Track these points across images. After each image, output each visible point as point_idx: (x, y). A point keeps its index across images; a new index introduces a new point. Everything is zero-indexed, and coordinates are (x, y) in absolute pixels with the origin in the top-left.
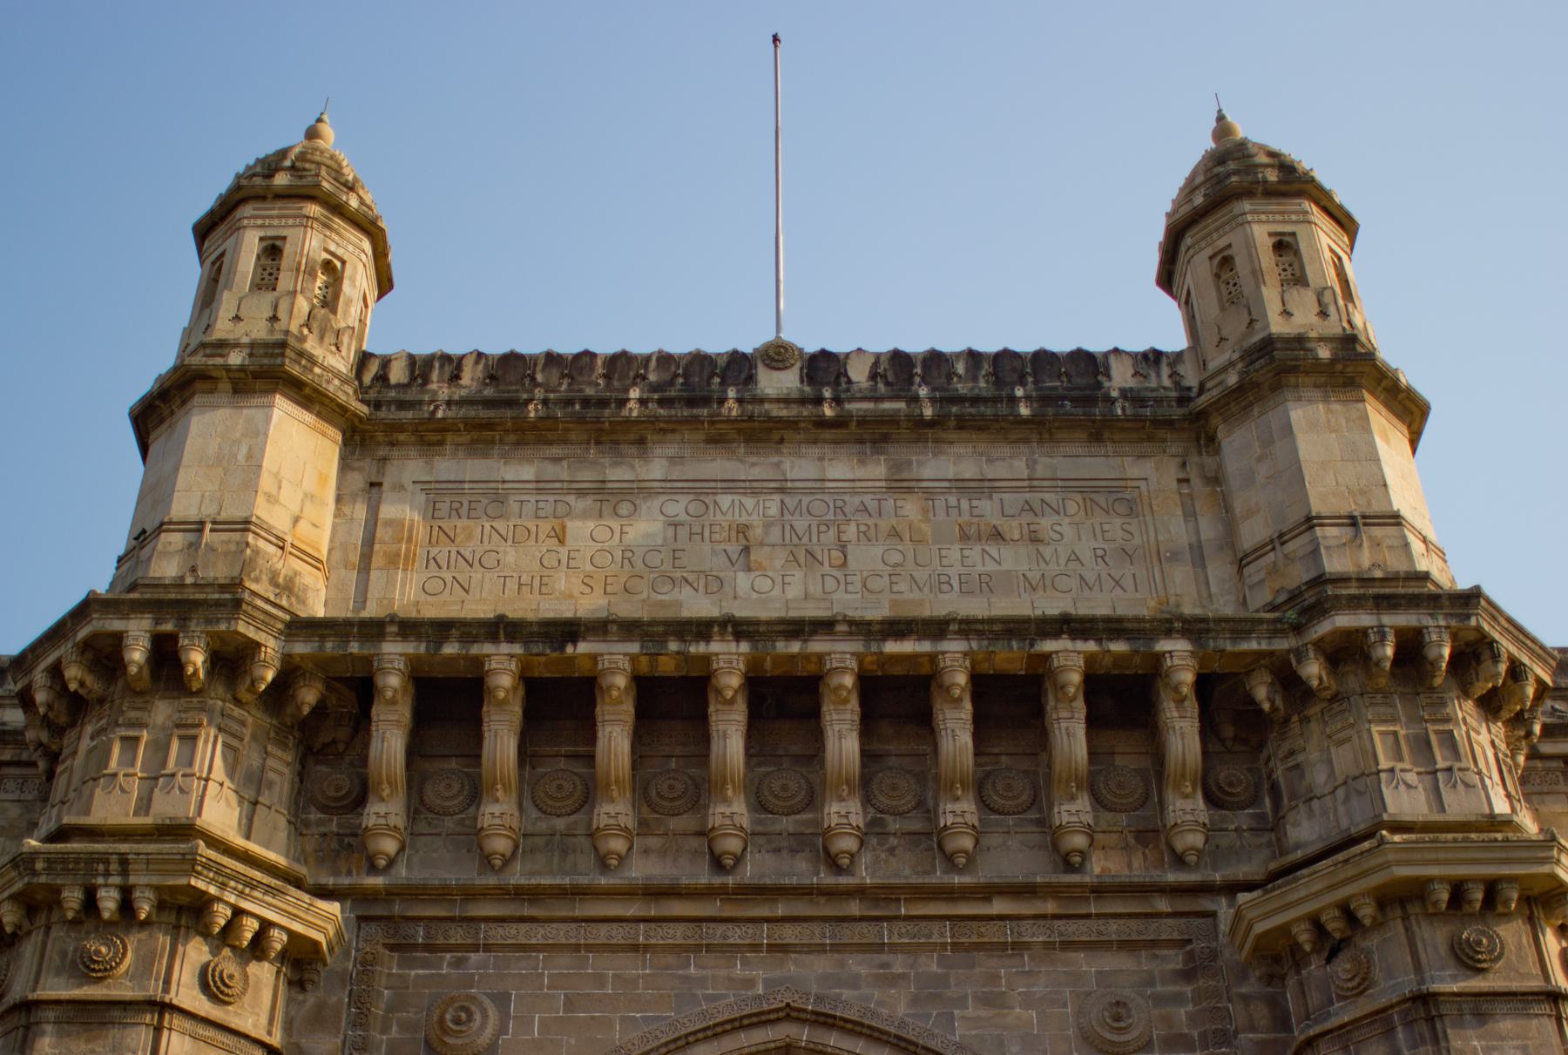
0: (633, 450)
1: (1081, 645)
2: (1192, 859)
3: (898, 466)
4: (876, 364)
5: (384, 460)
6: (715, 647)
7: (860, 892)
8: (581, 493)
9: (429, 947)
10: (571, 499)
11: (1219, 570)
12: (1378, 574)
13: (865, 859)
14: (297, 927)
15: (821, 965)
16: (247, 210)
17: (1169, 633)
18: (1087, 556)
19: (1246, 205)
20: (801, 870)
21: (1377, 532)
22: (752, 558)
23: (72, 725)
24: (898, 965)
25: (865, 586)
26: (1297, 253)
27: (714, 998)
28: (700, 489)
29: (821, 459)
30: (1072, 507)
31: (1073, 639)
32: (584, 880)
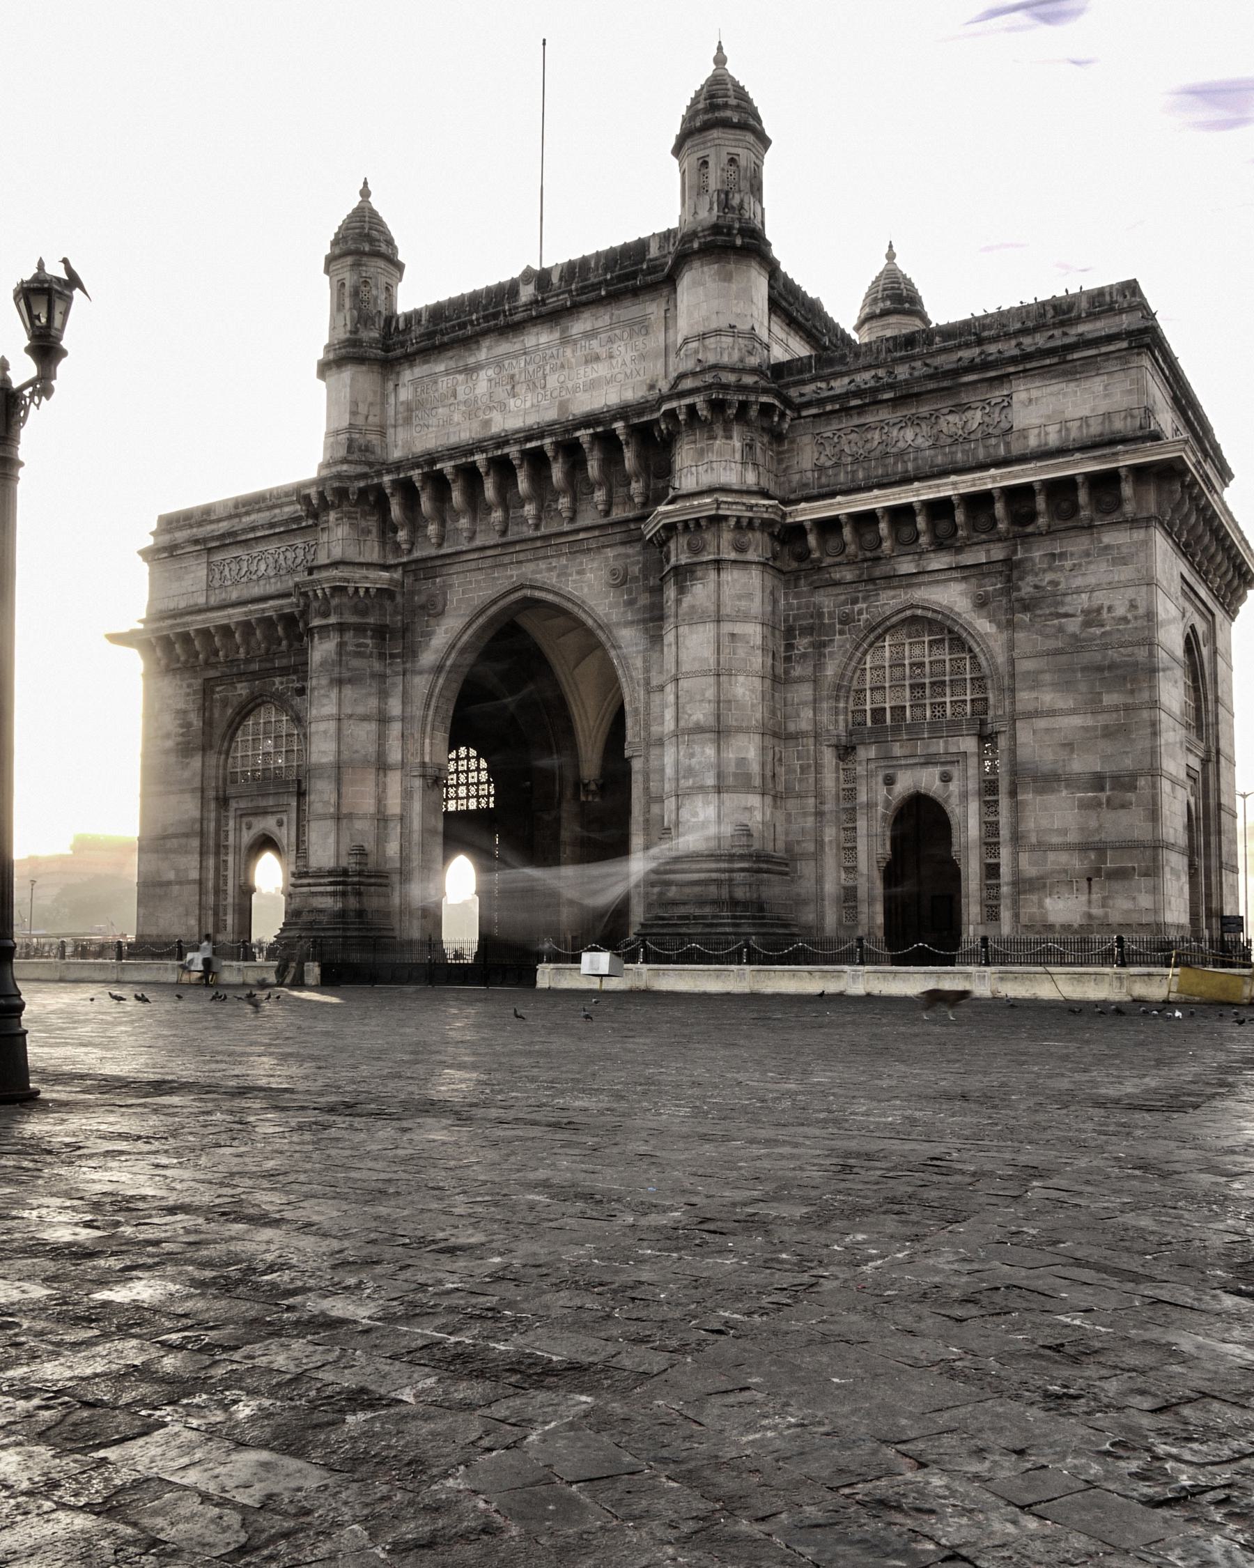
0: (474, 346)
3: (563, 331)
5: (398, 373)
6: (476, 457)
8: (460, 372)
13: (543, 523)
15: (531, 567)
17: (615, 419)
18: (628, 361)
19: (688, 144)
21: (707, 342)
24: (554, 562)
28: (498, 363)
30: (626, 335)
32: (459, 548)
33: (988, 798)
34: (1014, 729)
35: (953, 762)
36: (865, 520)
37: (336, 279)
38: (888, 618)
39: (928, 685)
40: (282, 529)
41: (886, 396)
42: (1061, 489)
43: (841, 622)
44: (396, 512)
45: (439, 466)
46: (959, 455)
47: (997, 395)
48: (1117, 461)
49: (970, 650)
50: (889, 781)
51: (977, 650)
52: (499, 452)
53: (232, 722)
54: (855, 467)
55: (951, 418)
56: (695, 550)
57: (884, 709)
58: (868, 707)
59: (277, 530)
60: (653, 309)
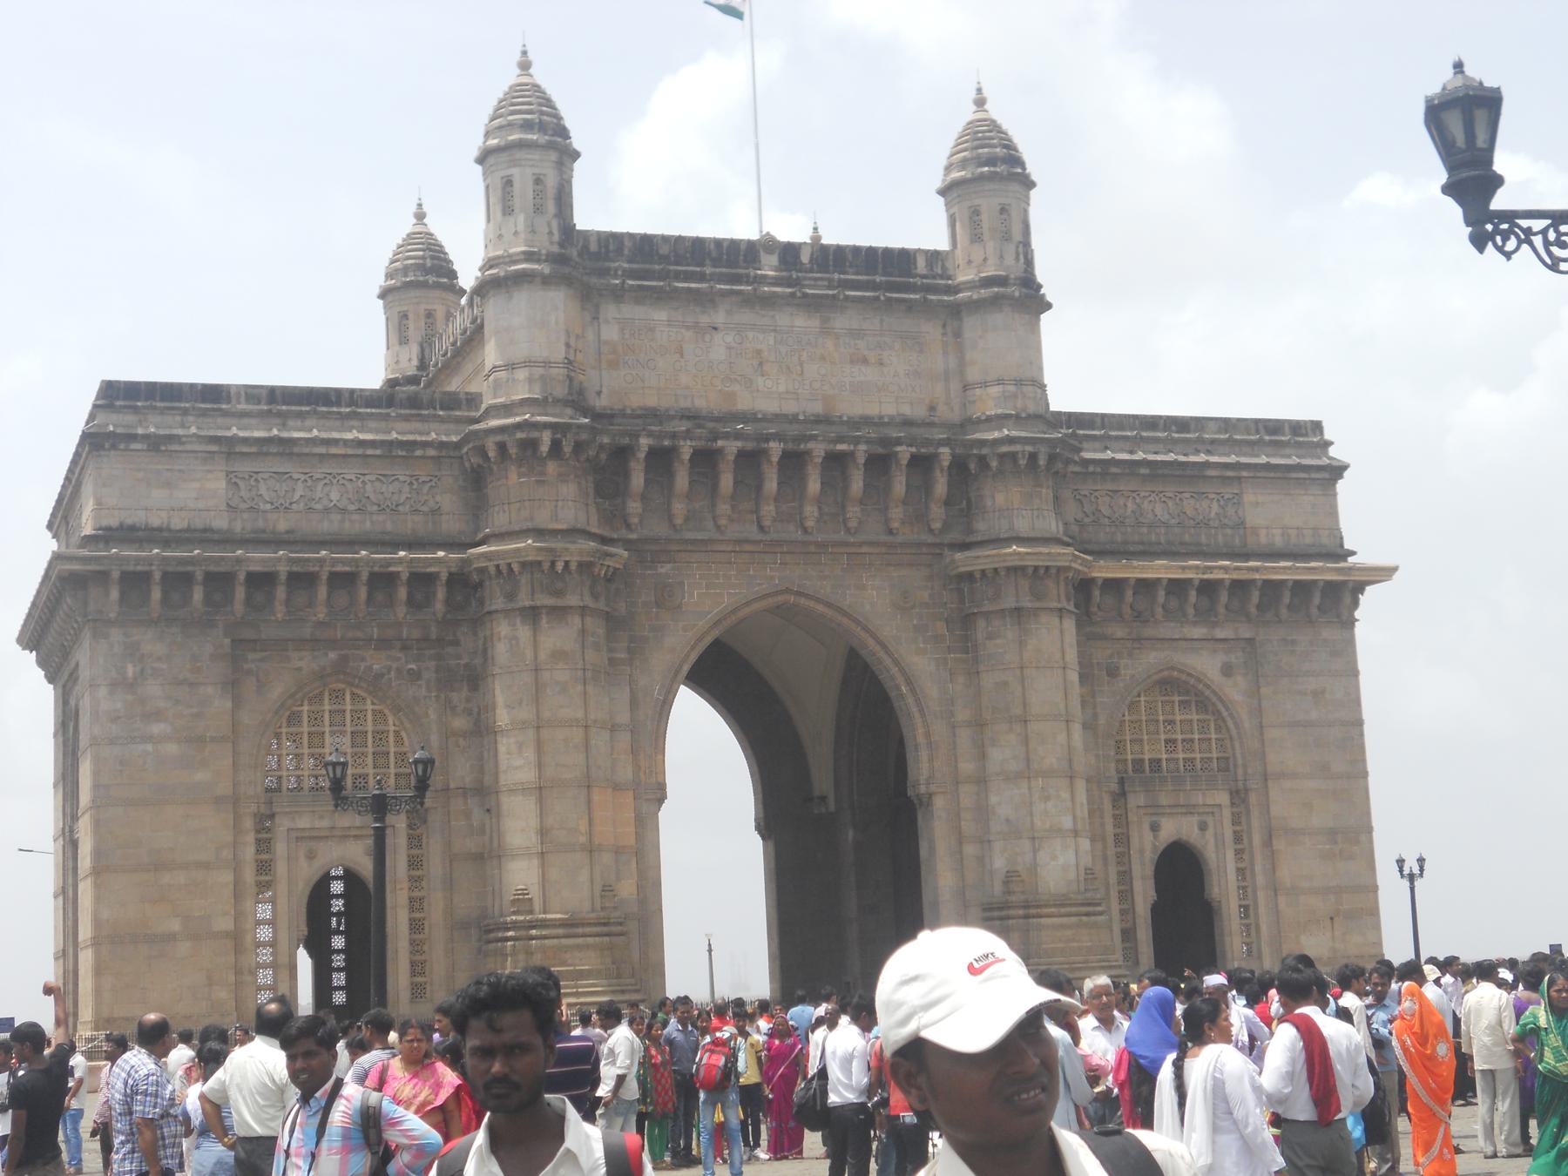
1: (910, 449)
2: (937, 532)
4: (812, 254)
5: (597, 307)
6: (772, 444)
7: (816, 544)
8: (688, 328)
9: (652, 562)
10: (683, 331)
11: (955, 386)
12: (1024, 415)
14: (617, 566)
16: (520, 155)
17: (941, 443)
20: (792, 532)
21: (1025, 389)
22: (764, 368)
23: (502, 463)
25: (811, 385)
26: (1009, 215)
27: (760, 584)
29: (792, 314)
31: (908, 446)
33: (1239, 847)
34: (1266, 787)
35: (1208, 813)
36: (1146, 586)
37: (529, 171)
38: (1149, 677)
39: (1180, 742)
40: (378, 452)
41: (1144, 471)
42: (1302, 589)
43: (1108, 675)
44: (638, 480)
45: (720, 443)
46: (1203, 537)
47: (1228, 491)
48: (1349, 575)
49: (1218, 711)
50: (1155, 828)
51: (1225, 714)
52: (802, 446)
53: (283, 704)
54: (1113, 529)
55: (1192, 501)
56: (1038, 596)
57: (1142, 760)
58: (1129, 757)
59: (370, 452)
60: (931, 330)
